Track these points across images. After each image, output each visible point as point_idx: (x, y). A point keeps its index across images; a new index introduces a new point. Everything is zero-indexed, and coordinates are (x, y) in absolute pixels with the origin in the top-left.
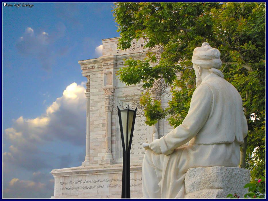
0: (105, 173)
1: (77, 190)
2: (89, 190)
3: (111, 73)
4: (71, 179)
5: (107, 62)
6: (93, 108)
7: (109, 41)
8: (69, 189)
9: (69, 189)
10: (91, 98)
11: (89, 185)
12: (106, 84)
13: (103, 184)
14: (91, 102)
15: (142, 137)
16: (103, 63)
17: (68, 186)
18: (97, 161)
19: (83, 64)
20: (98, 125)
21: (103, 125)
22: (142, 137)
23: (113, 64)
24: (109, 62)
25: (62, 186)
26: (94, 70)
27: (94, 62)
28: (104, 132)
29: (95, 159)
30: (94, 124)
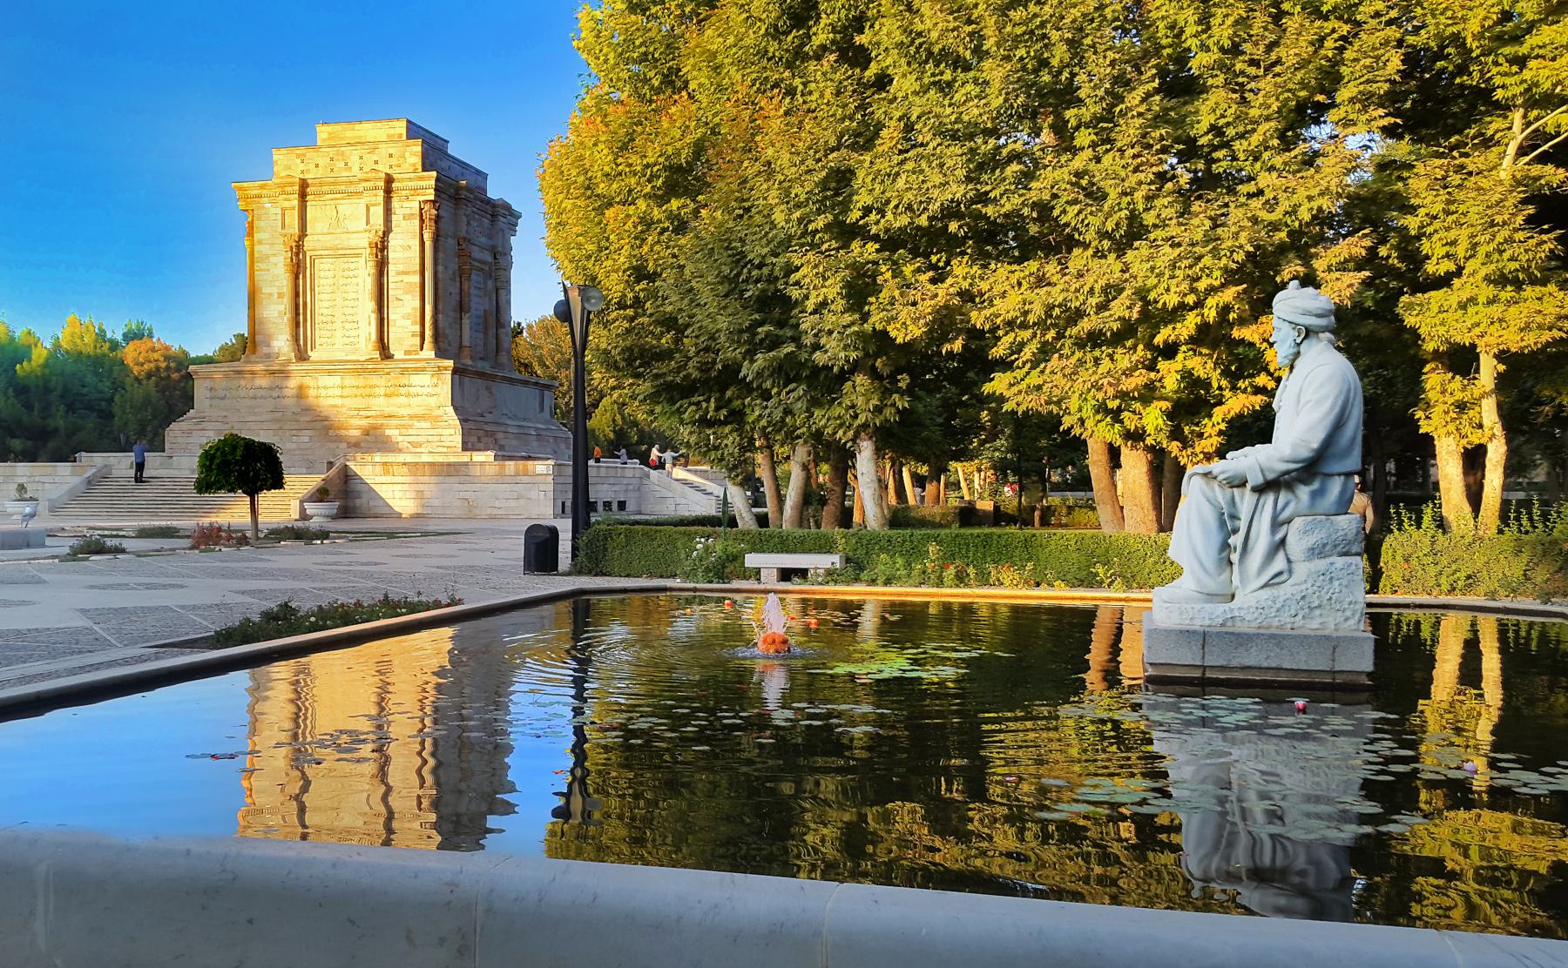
8: (222, 399)
12: (283, 227)
21: (280, 295)
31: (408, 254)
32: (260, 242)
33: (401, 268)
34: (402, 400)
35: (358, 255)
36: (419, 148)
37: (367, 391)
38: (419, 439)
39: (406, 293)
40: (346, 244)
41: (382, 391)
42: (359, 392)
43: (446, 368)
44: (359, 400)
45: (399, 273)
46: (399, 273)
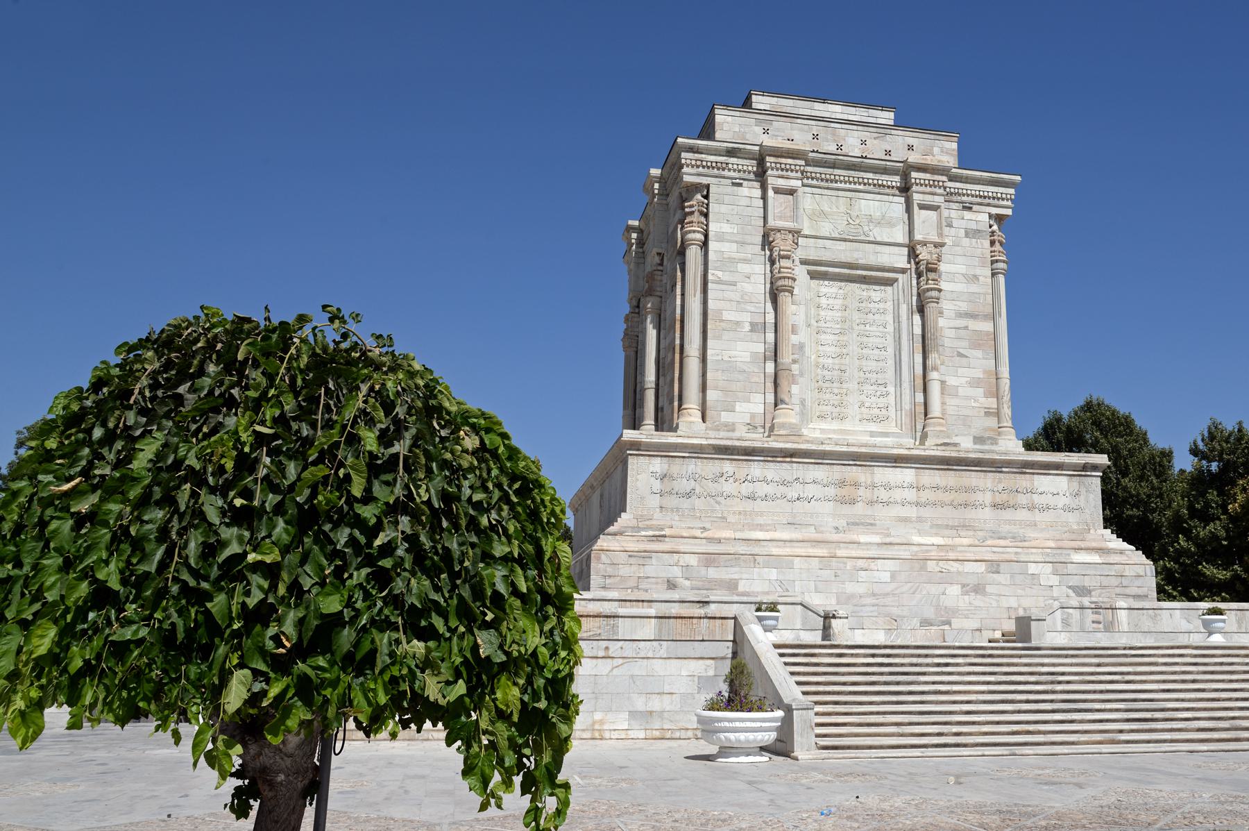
1: (718, 503)
2: (759, 505)
3: (791, 192)
4: (693, 466)
5: (783, 160)
7: (738, 114)
8: (688, 495)
9: (688, 495)
10: (712, 245)
11: (762, 489)
13: (811, 490)
14: (711, 256)
17: (684, 485)
19: (692, 149)
20: (738, 323)
21: (754, 327)
24: (790, 161)
25: (657, 486)
26: (726, 173)
27: (731, 153)
28: (760, 348)
29: (725, 417)
31: (974, 288)
32: (721, 238)
33: (964, 306)
34: (1023, 515)
35: (890, 282)
36: (955, 146)
37: (961, 497)
38: (1087, 582)
39: (975, 345)
40: (872, 260)
41: (988, 498)
42: (947, 497)
43: (1095, 467)
44: (948, 512)
45: (961, 315)
46: (961, 315)
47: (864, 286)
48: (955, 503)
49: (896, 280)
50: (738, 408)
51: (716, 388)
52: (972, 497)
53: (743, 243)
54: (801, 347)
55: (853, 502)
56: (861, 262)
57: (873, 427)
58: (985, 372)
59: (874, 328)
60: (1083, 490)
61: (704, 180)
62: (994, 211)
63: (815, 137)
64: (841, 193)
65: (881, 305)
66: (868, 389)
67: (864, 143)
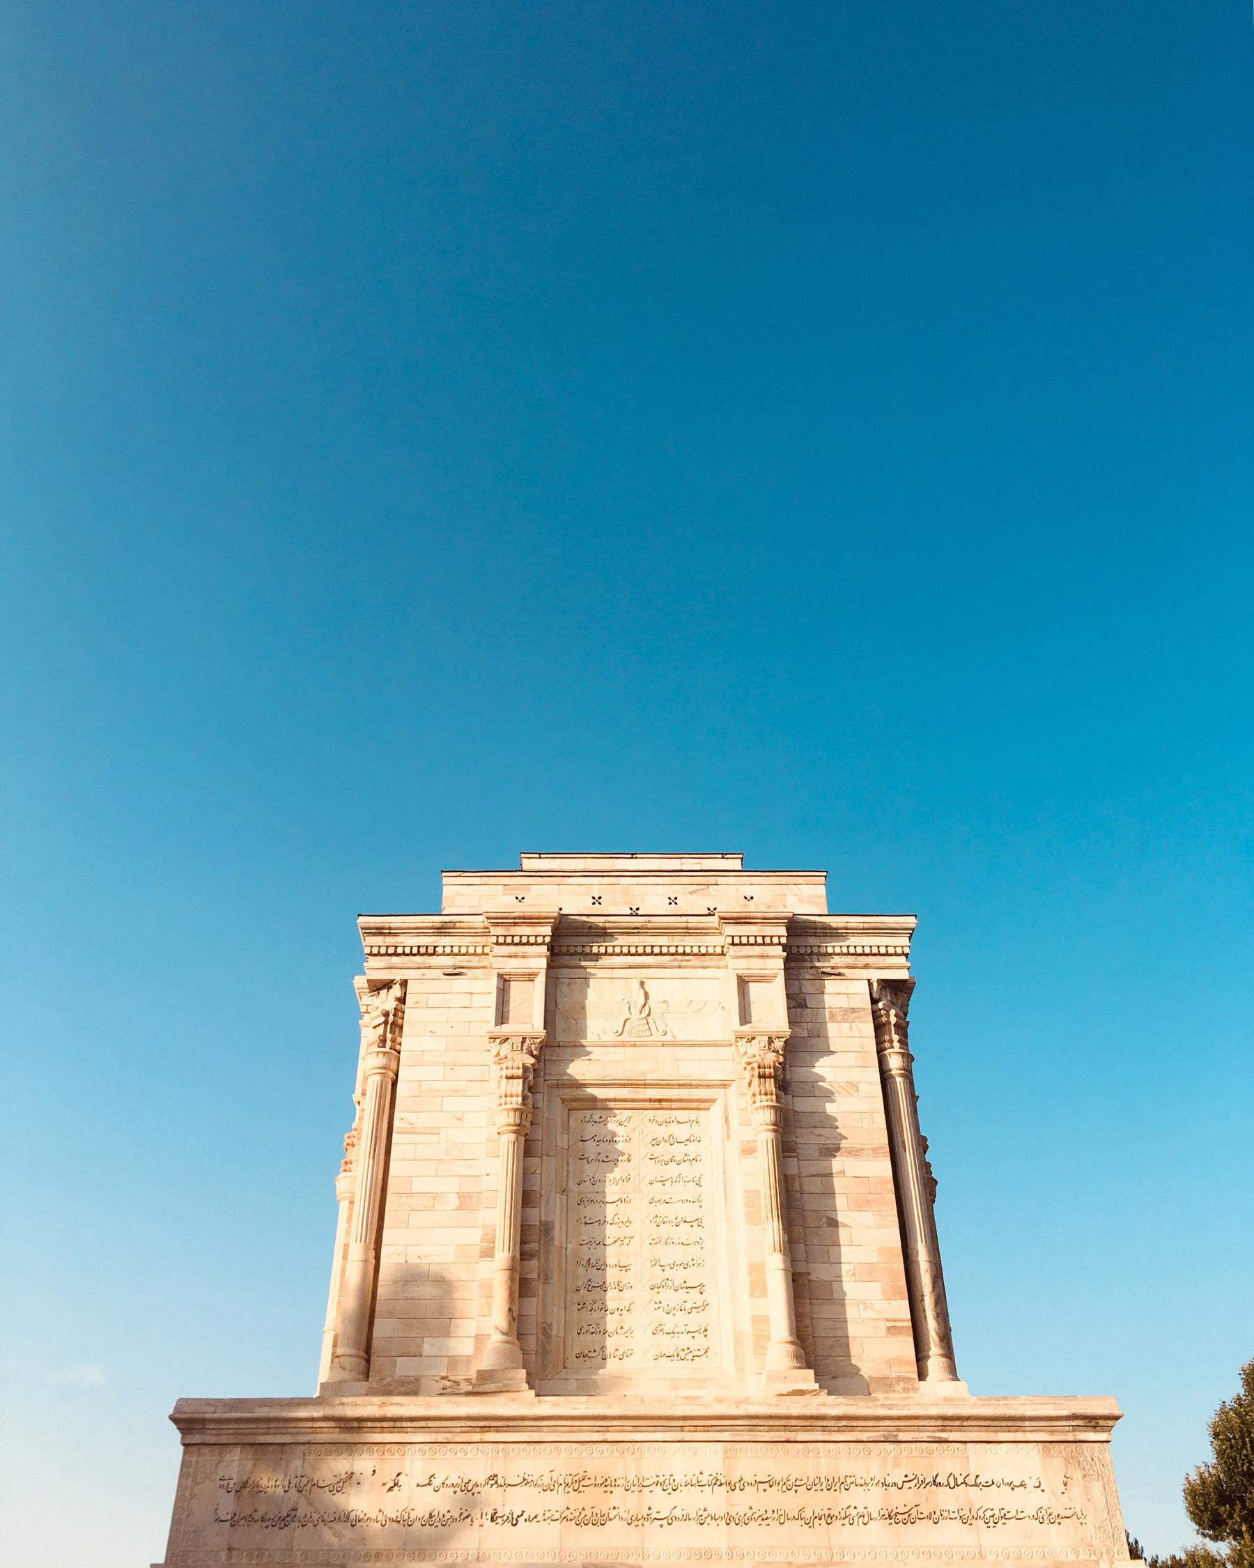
0: (536, 1436)
3: (531, 977)
6: (412, 1117)
7: (477, 880)
12: (502, 1018)
15: (678, 1276)
16: (500, 931)
18: (418, 1380)
19: (379, 931)
20: (435, 1197)
21: (466, 1201)
22: (678, 1276)
23: (547, 940)
24: (527, 930)
27: (441, 930)
28: (475, 1237)
29: (404, 1367)
30: (411, 1194)
34: (951, 1534)
36: (822, 890)
41: (873, 1500)
42: (790, 1502)
47: (661, 1115)
48: (808, 1514)
49: (713, 1101)
50: (427, 1349)
51: (391, 1315)
52: (843, 1500)
53: (453, 1066)
54: (547, 1229)
55: (600, 1520)
56: (649, 1076)
57: (678, 1369)
58: (881, 1251)
59: (679, 1187)
60: (1077, 1475)
61: (398, 975)
62: (876, 975)
63: (597, 900)
64: (617, 973)
65: (692, 1149)
66: (669, 1297)
67: (673, 901)
